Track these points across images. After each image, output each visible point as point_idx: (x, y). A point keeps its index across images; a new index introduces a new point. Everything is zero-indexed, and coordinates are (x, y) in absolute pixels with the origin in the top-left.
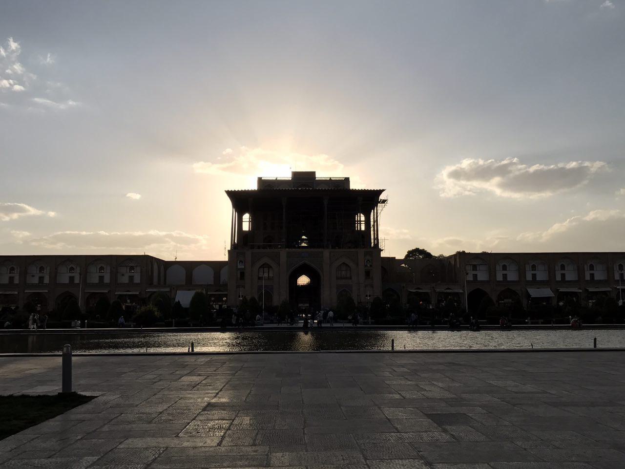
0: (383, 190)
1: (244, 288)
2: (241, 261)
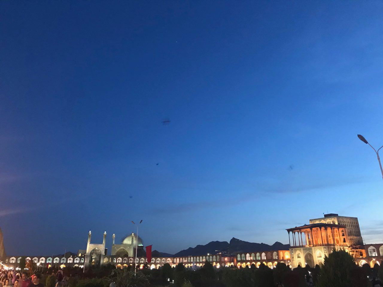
2: (292, 252)
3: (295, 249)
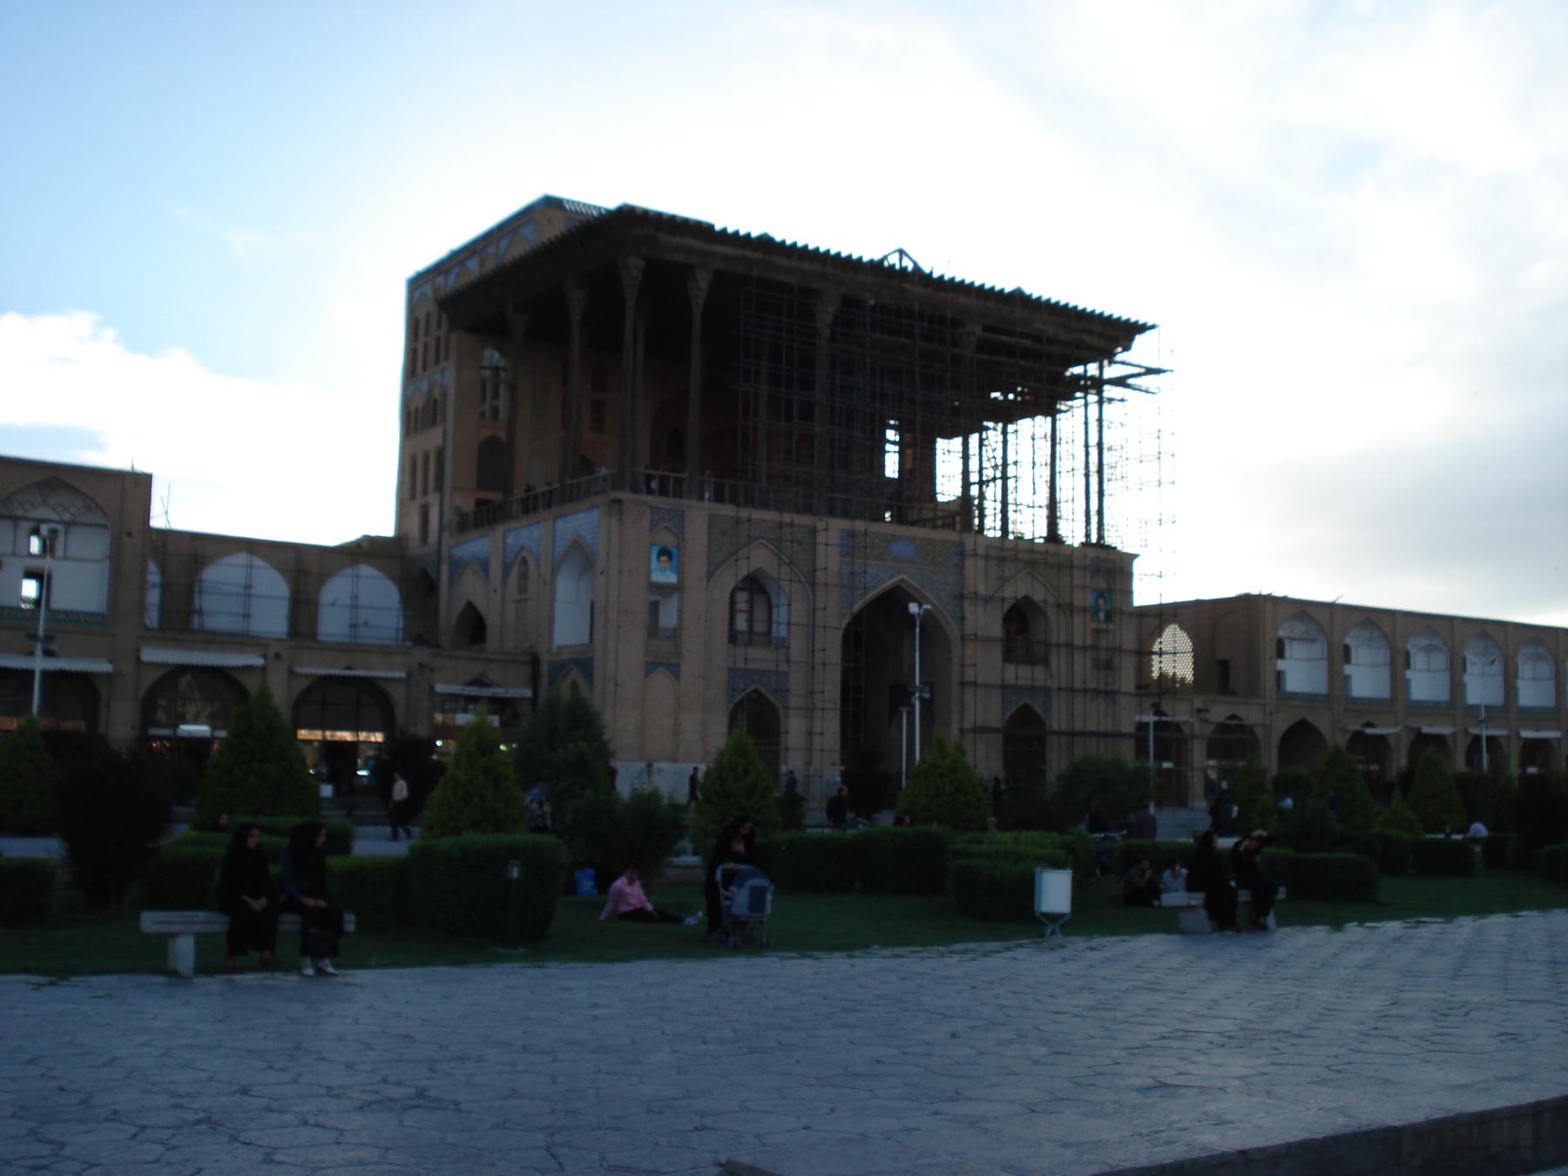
0: (1153, 327)
1: (677, 675)
2: (664, 552)
3: (713, 520)
